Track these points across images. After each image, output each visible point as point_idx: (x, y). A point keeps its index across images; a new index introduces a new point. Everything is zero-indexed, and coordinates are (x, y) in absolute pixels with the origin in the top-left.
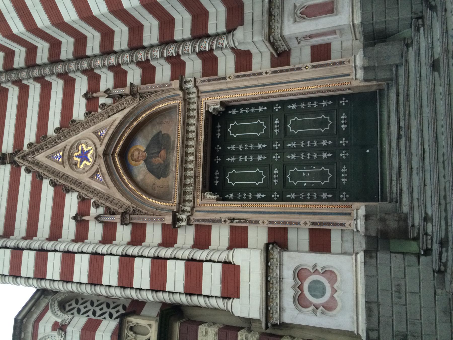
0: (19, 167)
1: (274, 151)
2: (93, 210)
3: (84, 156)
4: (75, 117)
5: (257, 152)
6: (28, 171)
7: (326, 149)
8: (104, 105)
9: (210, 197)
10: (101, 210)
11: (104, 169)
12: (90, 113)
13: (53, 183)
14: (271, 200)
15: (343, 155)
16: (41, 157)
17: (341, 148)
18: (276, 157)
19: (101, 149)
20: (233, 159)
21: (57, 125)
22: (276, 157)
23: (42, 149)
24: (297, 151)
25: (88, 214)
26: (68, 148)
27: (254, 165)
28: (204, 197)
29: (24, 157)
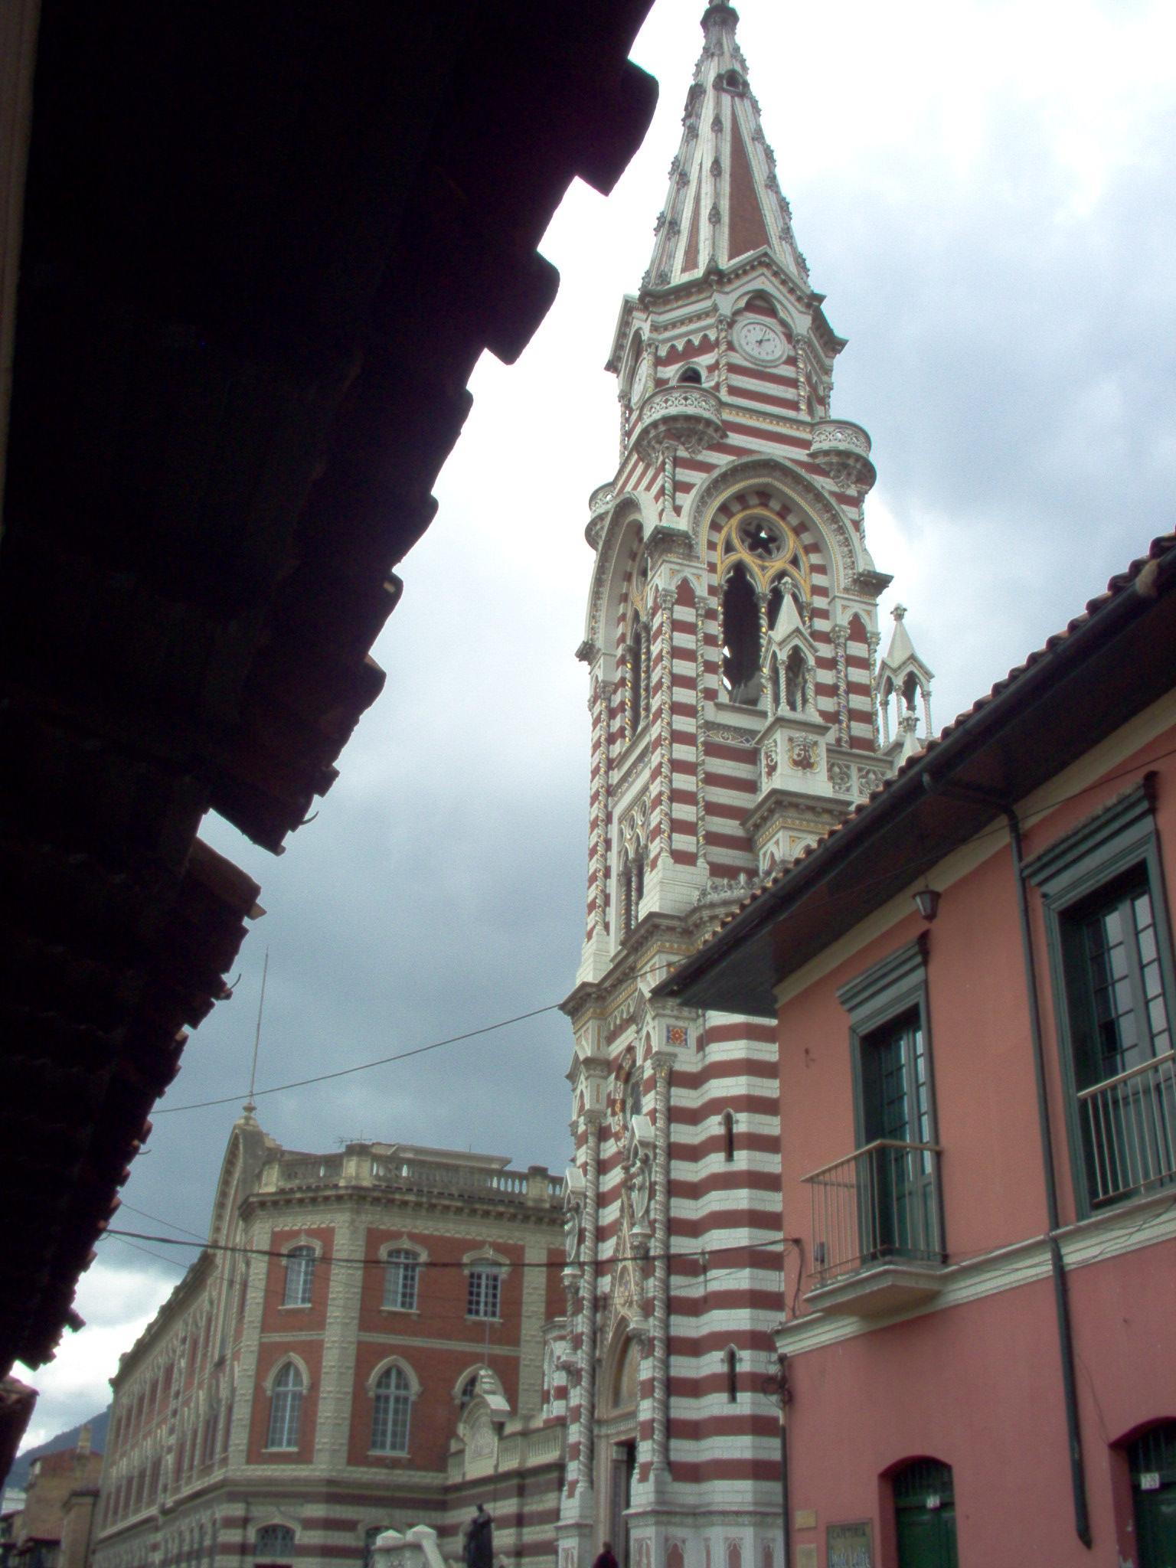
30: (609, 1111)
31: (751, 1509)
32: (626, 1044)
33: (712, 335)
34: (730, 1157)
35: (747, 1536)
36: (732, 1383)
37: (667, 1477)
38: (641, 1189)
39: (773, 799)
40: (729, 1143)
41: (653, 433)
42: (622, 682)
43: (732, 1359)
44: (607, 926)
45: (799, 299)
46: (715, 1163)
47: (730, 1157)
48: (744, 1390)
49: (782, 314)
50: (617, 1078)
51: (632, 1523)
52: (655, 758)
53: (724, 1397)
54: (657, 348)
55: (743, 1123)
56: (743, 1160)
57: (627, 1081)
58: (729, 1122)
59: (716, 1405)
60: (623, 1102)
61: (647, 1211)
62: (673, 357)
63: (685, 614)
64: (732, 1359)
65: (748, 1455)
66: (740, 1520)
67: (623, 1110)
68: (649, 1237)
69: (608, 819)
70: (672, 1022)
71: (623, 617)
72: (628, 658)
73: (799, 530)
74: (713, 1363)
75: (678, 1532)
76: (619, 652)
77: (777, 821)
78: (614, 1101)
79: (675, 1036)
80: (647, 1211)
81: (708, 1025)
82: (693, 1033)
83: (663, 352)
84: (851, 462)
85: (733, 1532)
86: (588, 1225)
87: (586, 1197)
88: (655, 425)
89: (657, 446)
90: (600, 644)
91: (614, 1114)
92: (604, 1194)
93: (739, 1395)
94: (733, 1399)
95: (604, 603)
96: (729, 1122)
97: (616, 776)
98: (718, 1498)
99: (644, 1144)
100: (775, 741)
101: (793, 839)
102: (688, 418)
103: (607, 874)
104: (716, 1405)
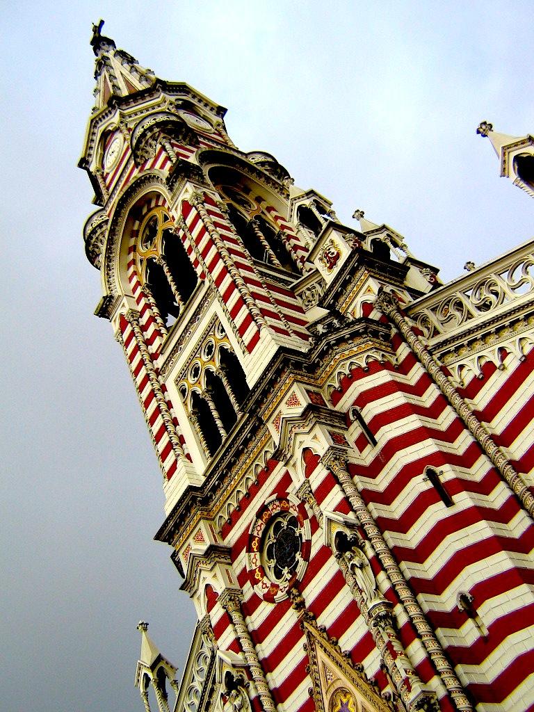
30: (248, 584)
32: (258, 506)
34: (449, 503)
38: (362, 567)
40: (442, 492)
41: (149, 134)
42: (147, 306)
44: (188, 456)
45: (212, 109)
46: (437, 512)
47: (449, 503)
49: (202, 113)
50: (250, 550)
54: (126, 125)
55: (448, 473)
56: (464, 501)
57: (261, 550)
58: (432, 476)
60: (262, 569)
61: (377, 588)
67: (264, 574)
68: (390, 606)
69: (163, 389)
70: (330, 428)
71: (135, 273)
73: (259, 200)
77: (362, 273)
78: (253, 572)
79: (338, 439)
80: (377, 588)
81: (367, 420)
82: (355, 432)
86: (262, 690)
87: (247, 668)
88: (151, 129)
89: (154, 142)
90: (117, 292)
91: (255, 582)
92: (265, 659)
95: (116, 271)
96: (432, 476)
97: (159, 363)
100: (332, 242)
103: (175, 422)
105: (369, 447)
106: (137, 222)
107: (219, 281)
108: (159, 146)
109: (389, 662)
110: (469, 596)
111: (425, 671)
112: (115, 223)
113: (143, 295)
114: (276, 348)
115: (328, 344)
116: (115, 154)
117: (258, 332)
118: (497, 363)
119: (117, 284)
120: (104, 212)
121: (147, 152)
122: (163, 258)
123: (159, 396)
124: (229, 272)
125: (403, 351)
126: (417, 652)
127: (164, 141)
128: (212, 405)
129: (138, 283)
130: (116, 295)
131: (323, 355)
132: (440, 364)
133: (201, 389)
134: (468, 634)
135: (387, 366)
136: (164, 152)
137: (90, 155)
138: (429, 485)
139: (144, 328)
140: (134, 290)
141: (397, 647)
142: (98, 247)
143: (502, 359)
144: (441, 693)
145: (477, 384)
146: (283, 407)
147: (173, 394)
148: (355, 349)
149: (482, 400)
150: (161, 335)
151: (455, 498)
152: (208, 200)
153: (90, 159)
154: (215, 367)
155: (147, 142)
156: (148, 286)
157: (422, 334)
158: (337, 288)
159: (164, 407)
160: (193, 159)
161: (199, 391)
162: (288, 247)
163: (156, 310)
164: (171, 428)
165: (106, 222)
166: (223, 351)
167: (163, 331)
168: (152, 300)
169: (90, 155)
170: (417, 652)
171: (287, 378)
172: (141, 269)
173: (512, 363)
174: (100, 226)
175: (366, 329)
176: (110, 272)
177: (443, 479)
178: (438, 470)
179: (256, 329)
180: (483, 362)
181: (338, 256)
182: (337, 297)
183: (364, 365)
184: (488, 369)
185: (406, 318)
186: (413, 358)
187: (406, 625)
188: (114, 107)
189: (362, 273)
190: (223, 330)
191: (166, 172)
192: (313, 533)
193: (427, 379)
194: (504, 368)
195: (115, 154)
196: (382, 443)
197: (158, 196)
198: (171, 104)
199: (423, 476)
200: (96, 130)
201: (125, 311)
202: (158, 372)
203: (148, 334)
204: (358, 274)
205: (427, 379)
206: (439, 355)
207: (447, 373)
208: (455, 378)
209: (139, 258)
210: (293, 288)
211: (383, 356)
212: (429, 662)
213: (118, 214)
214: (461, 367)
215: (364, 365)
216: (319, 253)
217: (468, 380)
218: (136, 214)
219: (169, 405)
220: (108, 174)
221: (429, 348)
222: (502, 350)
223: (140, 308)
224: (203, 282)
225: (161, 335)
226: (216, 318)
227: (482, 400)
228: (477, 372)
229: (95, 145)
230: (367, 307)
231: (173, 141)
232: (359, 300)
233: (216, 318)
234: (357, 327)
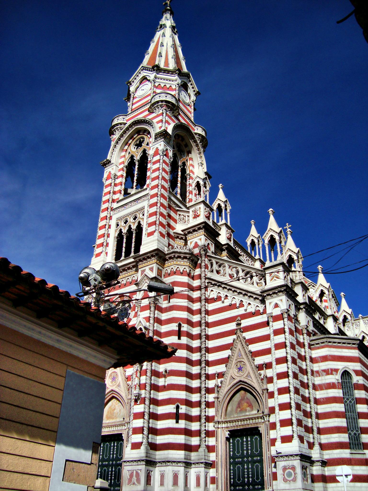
0: (236, 334)
1: (248, 458)
2: (219, 380)
3: (240, 369)
4: (257, 359)
5: (247, 450)
6: (234, 340)
7: (248, 480)
8: (260, 375)
9: (227, 434)
10: (220, 385)
11: (235, 382)
12: (258, 368)
13: (229, 356)
14: (230, 459)
15: (246, 487)
16: (239, 346)
17: (248, 486)
18: (245, 459)
19: (242, 379)
20: (245, 440)
21: (253, 350)
22: (245, 459)
23: (243, 345)
24: (248, 468)
25: (218, 378)
26: (243, 360)
27: (243, 450)
28: (226, 431)
29: (238, 337)
31: (185, 461)
33: (174, 87)
35: (181, 470)
36: (177, 416)
37: (149, 448)
39: (203, 225)
42: (122, 176)
43: (178, 407)
44: (107, 253)
47: (179, 338)
48: (182, 419)
51: (124, 464)
52: (154, 200)
53: (175, 421)
55: (185, 328)
58: (180, 326)
59: (170, 423)
62: (159, 87)
63: (165, 158)
64: (178, 407)
65: (183, 442)
66: (174, 464)
69: (111, 218)
71: (124, 156)
72: (125, 169)
74: (171, 409)
75: (151, 468)
76: (122, 166)
83: (157, 84)
84: (204, 140)
85: (176, 469)
88: (162, 101)
93: (180, 421)
94: (177, 422)
96: (180, 326)
97: (115, 205)
98: (170, 456)
99: (145, 328)
100: (200, 208)
101: (206, 240)
102: (173, 104)
104: (170, 423)
105: (166, 302)
106: (136, 135)
107: (152, 197)
108: (161, 112)
109: (134, 376)
110: (168, 372)
111: (142, 387)
112: (128, 129)
113: (123, 169)
114: (155, 248)
115: (174, 256)
116: (144, 92)
117: (155, 231)
118: (223, 299)
119: (115, 156)
120: (126, 117)
121: (155, 109)
122: (138, 161)
123: (108, 221)
124: (157, 197)
125: (197, 272)
126: (143, 379)
127: (164, 111)
128: (125, 240)
129: (123, 163)
130: (112, 162)
131: (170, 258)
132: (206, 284)
133: (124, 231)
134: (161, 382)
135: (189, 275)
136: (161, 116)
137: (133, 82)
138: (177, 329)
139: (116, 185)
140: (121, 164)
141: (138, 374)
142: (115, 131)
143: (225, 299)
144: (143, 396)
145: (214, 300)
146: (147, 268)
147: (113, 223)
148: (182, 263)
149: (211, 307)
150: (121, 193)
151: (182, 338)
152: (167, 155)
153: (133, 84)
154: (134, 227)
155: (157, 106)
156: (126, 167)
157: (208, 269)
158: (191, 230)
159: (107, 227)
160: (170, 131)
161: (123, 231)
162: (188, 183)
163: (124, 180)
164: (106, 237)
165: (125, 124)
166: (139, 222)
167: (123, 192)
168: (125, 175)
169: (133, 82)
170: (143, 379)
171: (154, 260)
172: (128, 156)
173: (227, 303)
174: (121, 124)
175: (190, 257)
176: (115, 149)
177: (182, 329)
178: (183, 325)
179: (154, 229)
180: (219, 295)
181: (198, 216)
182: (189, 233)
183: (181, 271)
184: (219, 299)
185: (206, 259)
186: (200, 277)
187: (144, 370)
188: (154, 70)
189: (202, 232)
190: (143, 215)
191: (158, 130)
192: (134, 317)
193: (199, 288)
194: (223, 302)
195: (144, 92)
196: (171, 304)
197: (149, 133)
198: (178, 84)
199: (177, 324)
200: (142, 72)
201: (113, 172)
202: (112, 209)
203: (117, 189)
204: (201, 231)
205: (199, 288)
206: (208, 281)
207: (206, 290)
208: (208, 293)
209: (129, 150)
210: (178, 210)
211: (190, 270)
212: (145, 385)
213: (131, 126)
214: (212, 291)
215: (181, 271)
216: (193, 209)
217: (211, 297)
218: (138, 132)
219: (110, 227)
220: (136, 98)
221: (206, 276)
222: (227, 296)
223: (119, 174)
224: (146, 189)
225: (121, 193)
226: (143, 208)
227: (211, 307)
228: (215, 297)
229: (139, 78)
230: (196, 245)
231: (168, 113)
232: (196, 240)
233: (143, 208)
234: (187, 255)
